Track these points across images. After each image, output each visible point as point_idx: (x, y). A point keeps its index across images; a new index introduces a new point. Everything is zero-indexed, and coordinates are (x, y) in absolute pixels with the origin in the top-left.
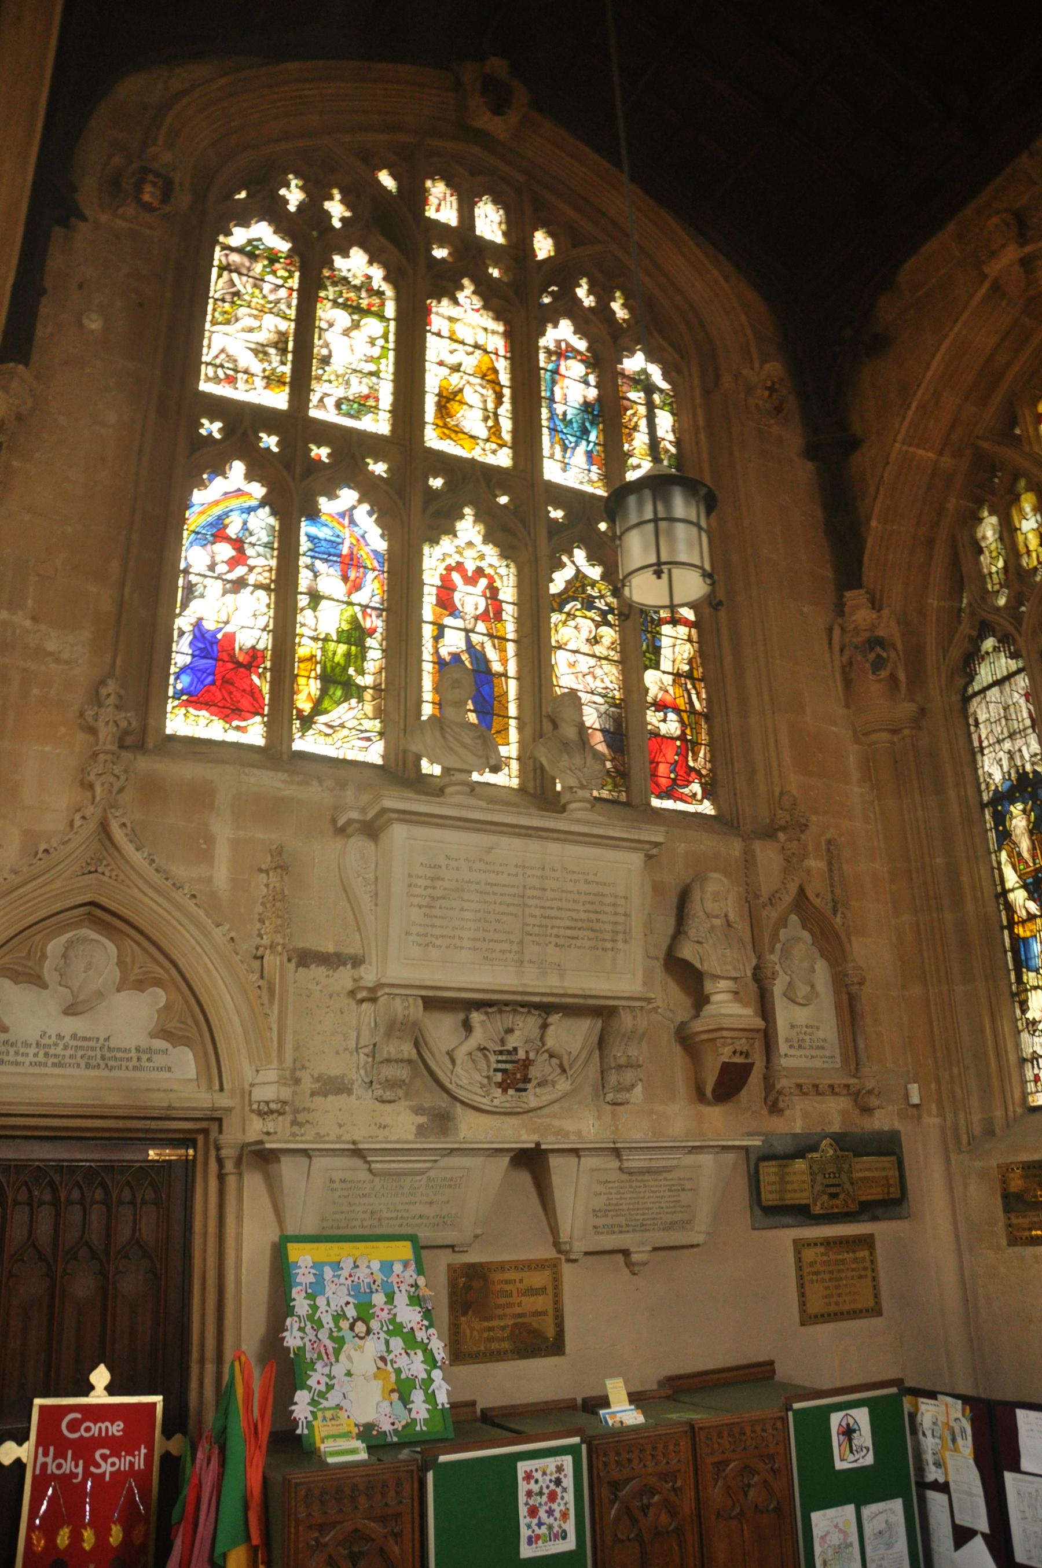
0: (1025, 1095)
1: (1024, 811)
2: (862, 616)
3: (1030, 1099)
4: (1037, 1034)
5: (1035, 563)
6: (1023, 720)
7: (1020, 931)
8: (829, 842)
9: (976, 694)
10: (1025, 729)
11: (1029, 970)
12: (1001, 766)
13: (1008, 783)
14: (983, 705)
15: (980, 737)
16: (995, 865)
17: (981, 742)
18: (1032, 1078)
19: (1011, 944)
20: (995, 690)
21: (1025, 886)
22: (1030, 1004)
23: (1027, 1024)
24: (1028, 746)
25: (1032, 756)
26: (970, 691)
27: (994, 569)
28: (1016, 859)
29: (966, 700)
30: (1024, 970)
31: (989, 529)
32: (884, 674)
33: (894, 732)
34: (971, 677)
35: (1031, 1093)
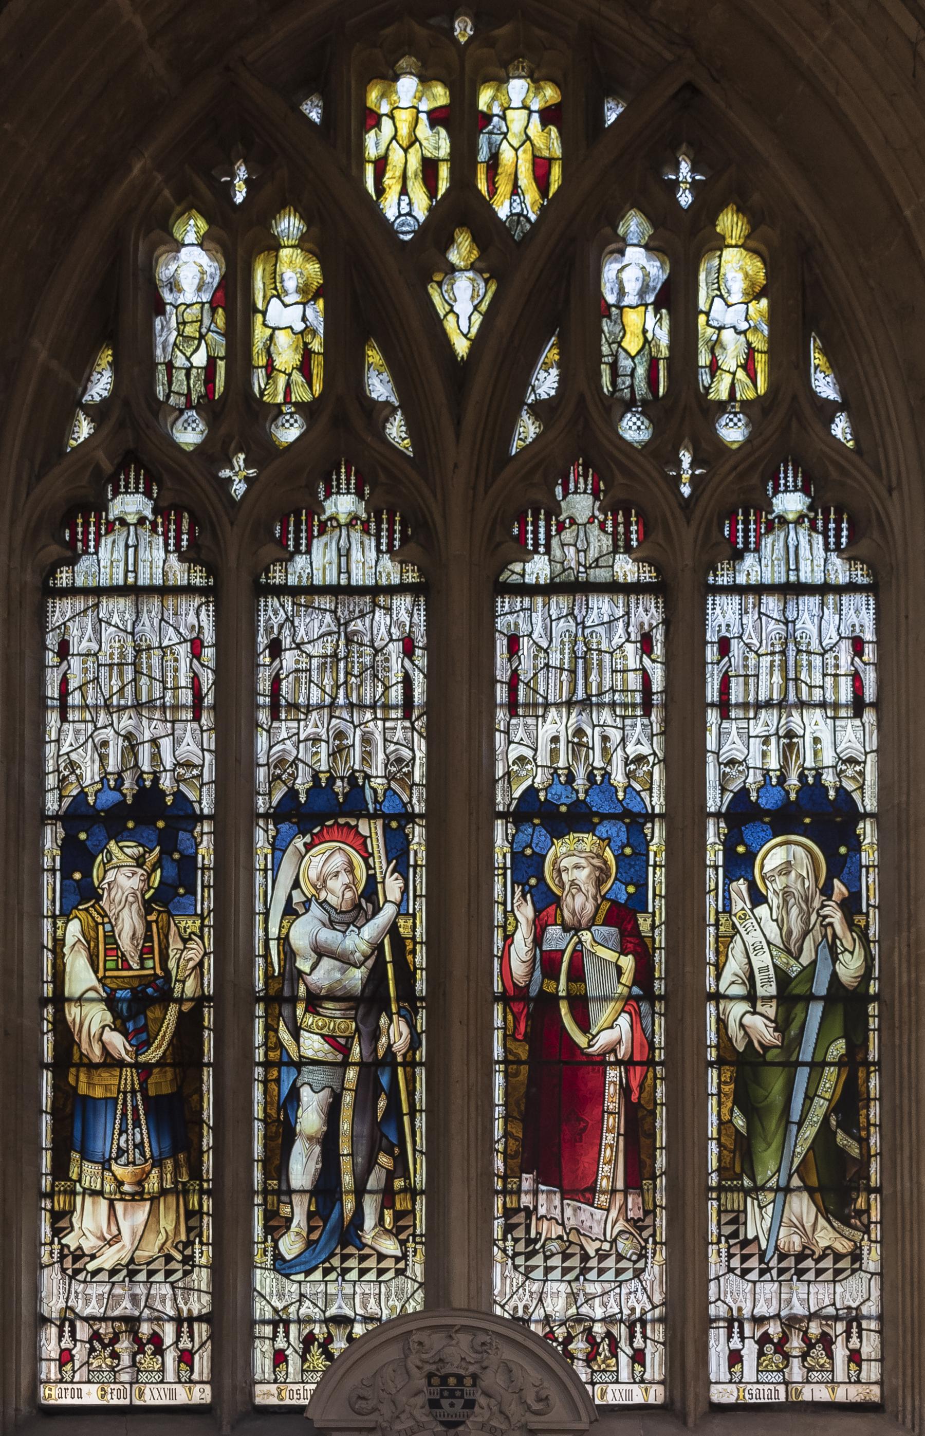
1: (140, 862)
4: (81, 1277)
6: (176, 688)
9: (73, 591)
14: (88, 621)
15: (64, 682)
16: (48, 941)
17: (64, 692)
21: (110, 1002)
24: (176, 743)
25: (178, 764)
26: (63, 578)
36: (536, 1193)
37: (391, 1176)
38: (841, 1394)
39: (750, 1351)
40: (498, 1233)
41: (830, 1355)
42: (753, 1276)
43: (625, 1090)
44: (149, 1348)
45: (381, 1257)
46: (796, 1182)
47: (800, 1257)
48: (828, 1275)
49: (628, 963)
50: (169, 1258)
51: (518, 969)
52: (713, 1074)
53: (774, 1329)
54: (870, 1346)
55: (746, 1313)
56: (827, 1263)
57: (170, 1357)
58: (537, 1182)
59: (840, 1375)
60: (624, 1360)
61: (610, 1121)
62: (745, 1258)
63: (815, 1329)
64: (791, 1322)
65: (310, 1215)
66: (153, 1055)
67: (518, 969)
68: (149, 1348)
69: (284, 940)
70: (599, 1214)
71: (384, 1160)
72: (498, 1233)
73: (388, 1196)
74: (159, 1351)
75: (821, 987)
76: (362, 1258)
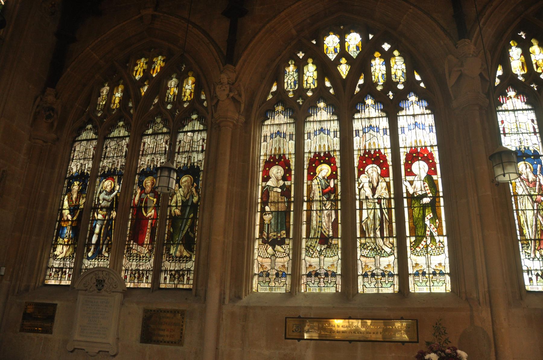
0: (44, 279)
2: (50, 98)
3: (46, 281)
4: (56, 260)
5: (115, 108)
6: (90, 155)
7: (63, 224)
8: (4, 171)
10: (89, 158)
11: (61, 237)
12: (77, 167)
13: (77, 174)
14: (79, 145)
15: (74, 155)
16: (62, 199)
17: (73, 157)
18: (49, 274)
19: (58, 227)
20: (85, 142)
21: (69, 209)
22: (57, 249)
23: (54, 256)
24: (88, 164)
25: (88, 168)
26: (77, 139)
27: (101, 103)
28: (70, 200)
29: (74, 141)
30: (59, 237)
31: (105, 90)
32: (49, 121)
33: (44, 142)
34: (79, 134)
35: (47, 279)
36: (133, 244)
37: (109, 241)
38: (185, 287)
39: (168, 277)
40: (125, 252)
41: (184, 278)
42: (171, 261)
43: (152, 224)
44: (64, 274)
45: (105, 257)
46: (181, 242)
47: (180, 257)
48: (185, 262)
49: (155, 200)
50: (70, 256)
51: (136, 201)
52: (168, 221)
53: (173, 272)
54: (191, 277)
55: (169, 269)
56: (185, 259)
57: (67, 275)
58: (133, 242)
59: (185, 282)
60: (145, 278)
61: (148, 230)
62: (169, 258)
63: (181, 273)
64: (177, 271)
65: (94, 249)
66: (75, 218)
67: (136, 201)
68: (64, 274)
69: (98, 198)
70: (144, 248)
71: (108, 238)
72: (125, 252)
73: (108, 245)
74: (65, 274)
75: (190, 204)
76: (102, 257)
